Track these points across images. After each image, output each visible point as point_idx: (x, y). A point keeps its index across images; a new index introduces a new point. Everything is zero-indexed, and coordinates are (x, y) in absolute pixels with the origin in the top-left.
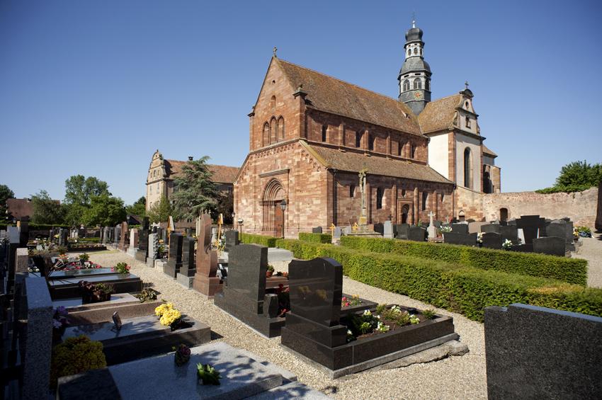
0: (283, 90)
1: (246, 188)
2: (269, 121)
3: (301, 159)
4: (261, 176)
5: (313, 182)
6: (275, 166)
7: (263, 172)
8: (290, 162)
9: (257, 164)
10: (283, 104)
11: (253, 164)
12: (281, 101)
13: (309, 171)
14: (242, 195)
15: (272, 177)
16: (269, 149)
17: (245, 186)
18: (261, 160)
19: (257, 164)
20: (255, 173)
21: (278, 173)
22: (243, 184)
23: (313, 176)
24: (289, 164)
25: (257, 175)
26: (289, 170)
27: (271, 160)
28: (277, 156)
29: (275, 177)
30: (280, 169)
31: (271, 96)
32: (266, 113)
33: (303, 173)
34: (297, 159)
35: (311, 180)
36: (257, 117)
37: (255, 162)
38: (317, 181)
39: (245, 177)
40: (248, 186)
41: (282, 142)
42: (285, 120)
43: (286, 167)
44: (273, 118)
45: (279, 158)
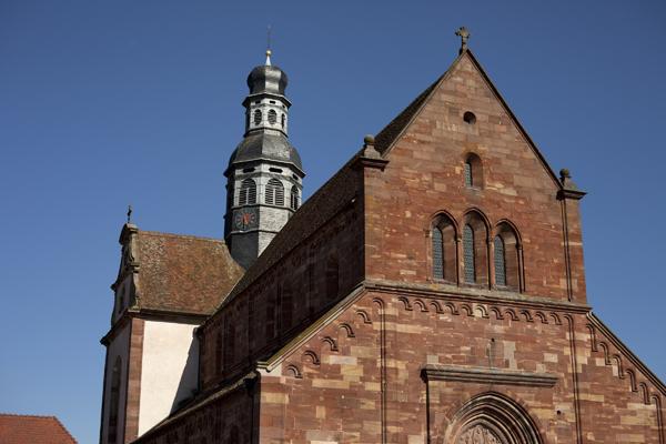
0: (508, 157)
1: (343, 404)
2: (457, 214)
3: (592, 362)
4: (425, 374)
5: (635, 429)
6: (492, 356)
7: (433, 361)
8: (553, 358)
9: (401, 328)
10: (511, 192)
11: (377, 326)
12: (508, 183)
13: (620, 399)
14: (311, 422)
15: (486, 387)
16: (470, 298)
17: (331, 396)
18: (424, 323)
19: (401, 328)
20: (397, 357)
21: (515, 381)
22: (317, 383)
23: (633, 413)
24: (550, 365)
25: (401, 365)
26: (548, 383)
27: (479, 332)
28: (499, 329)
29: (500, 388)
30: (513, 369)
31: (462, 150)
32: (440, 187)
33: (602, 399)
34: (583, 358)
35: (629, 421)
36: (398, 182)
37: (394, 319)
38: (646, 427)
39: (332, 359)
40: (354, 393)
41: (532, 299)
42: (526, 240)
43: (541, 370)
44: (476, 216)
45: (508, 336)
